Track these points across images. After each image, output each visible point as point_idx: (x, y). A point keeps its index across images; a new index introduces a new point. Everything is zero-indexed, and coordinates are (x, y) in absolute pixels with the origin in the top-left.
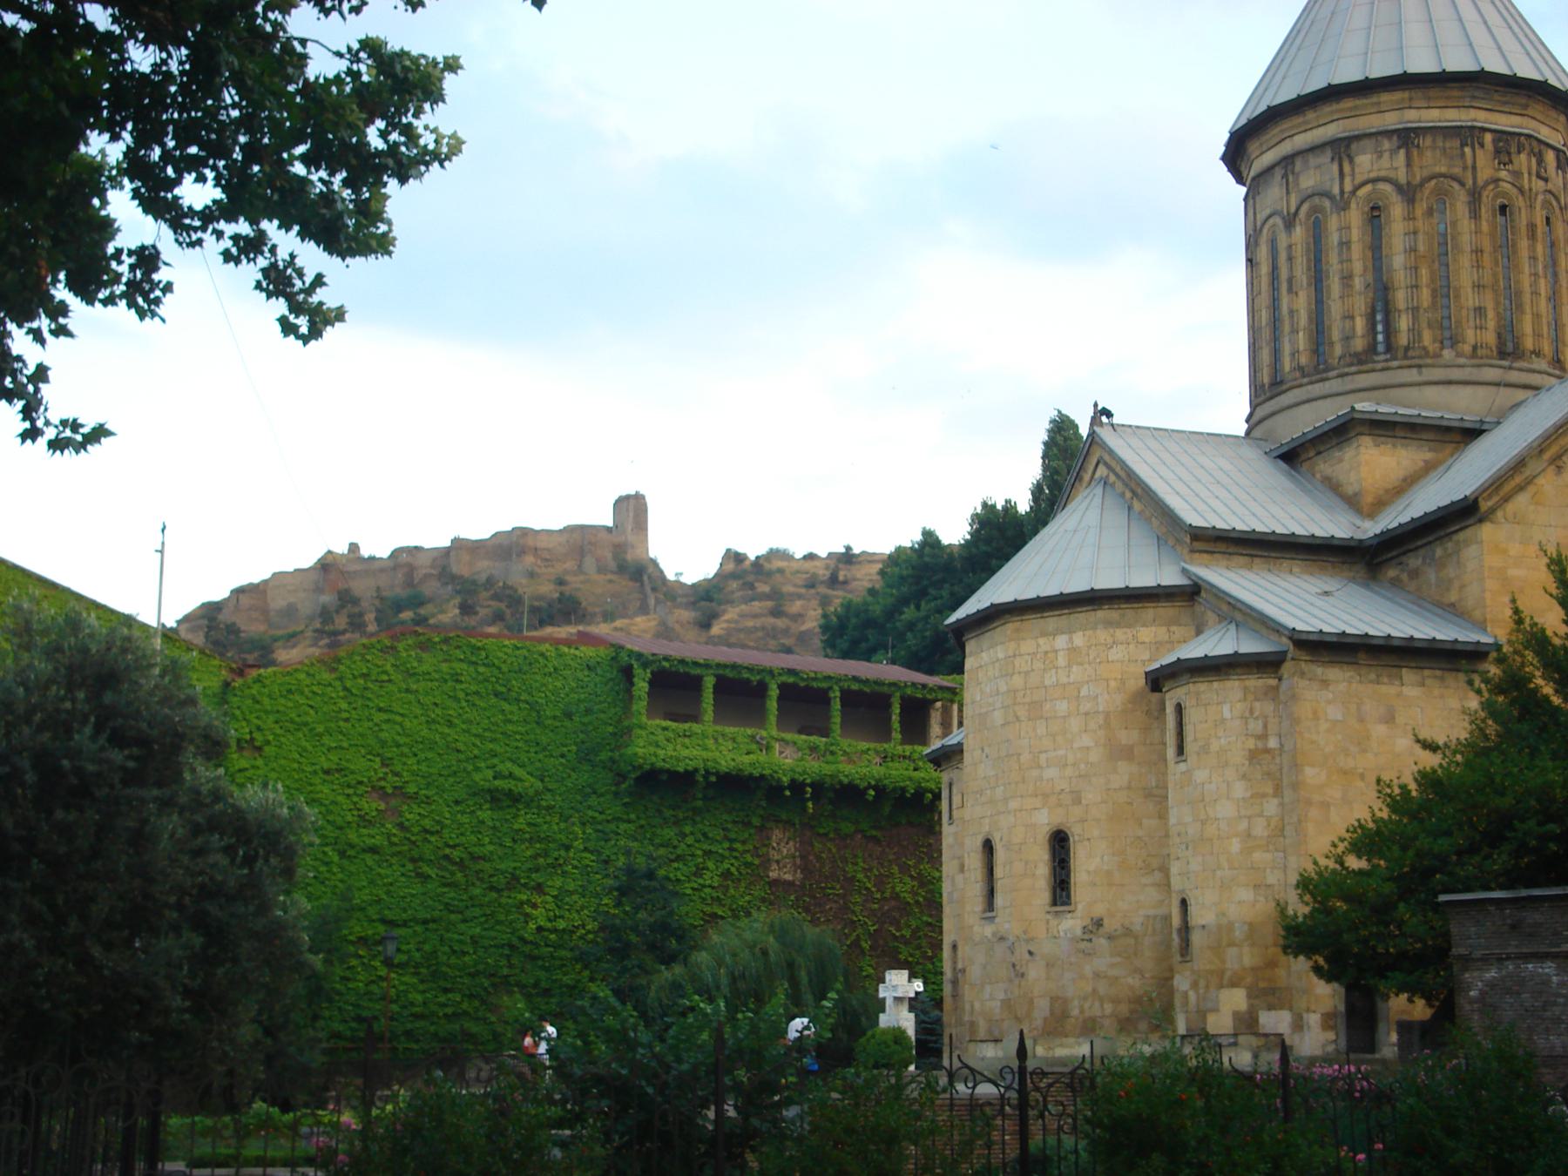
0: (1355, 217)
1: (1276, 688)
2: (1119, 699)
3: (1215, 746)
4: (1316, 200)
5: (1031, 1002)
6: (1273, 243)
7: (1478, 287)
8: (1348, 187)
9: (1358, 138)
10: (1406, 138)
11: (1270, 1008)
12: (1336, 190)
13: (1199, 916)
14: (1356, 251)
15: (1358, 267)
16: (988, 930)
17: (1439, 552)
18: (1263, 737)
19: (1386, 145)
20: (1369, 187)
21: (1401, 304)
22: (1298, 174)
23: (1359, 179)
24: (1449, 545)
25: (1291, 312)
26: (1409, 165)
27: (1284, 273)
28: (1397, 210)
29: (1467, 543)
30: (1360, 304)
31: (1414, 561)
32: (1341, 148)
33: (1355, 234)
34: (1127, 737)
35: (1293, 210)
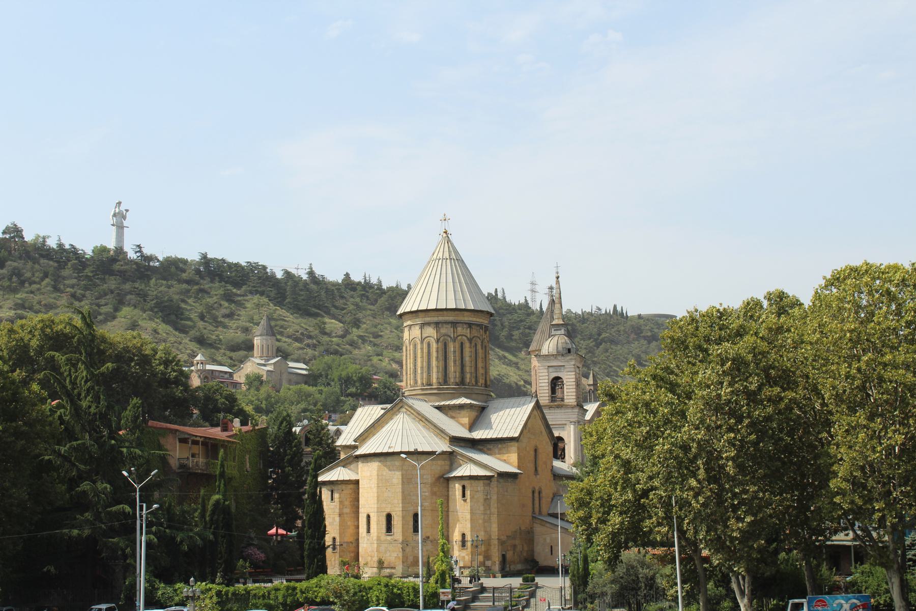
0: (457, 345)
1: (489, 485)
2: (434, 479)
3: (476, 497)
4: (446, 337)
5: (407, 557)
6: (429, 345)
7: (482, 368)
8: (455, 336)
9: (458, 323)
10: (470, 325)
11: (488, 560)
12: (452, 336)
13: (468, 538)
14: (457, 353)
15: (457, 359)
16: (389, 538)
17: (500, 446)
18: (487, 495)
19: (465, 326)
20: (460, 337)
21: (468, 371)
22: (440, 328)
23: (458, 334)
24: (504, 445)
25: (438, 367)
26: (470, 333)
27: (434, 354)
28: (467, 345)
29: (511, 446)
30: (458, 369)
31: (489, 446)
32: (454, 324)
33: (457, 348)
34: (435, 489)
35: (438, 338)
